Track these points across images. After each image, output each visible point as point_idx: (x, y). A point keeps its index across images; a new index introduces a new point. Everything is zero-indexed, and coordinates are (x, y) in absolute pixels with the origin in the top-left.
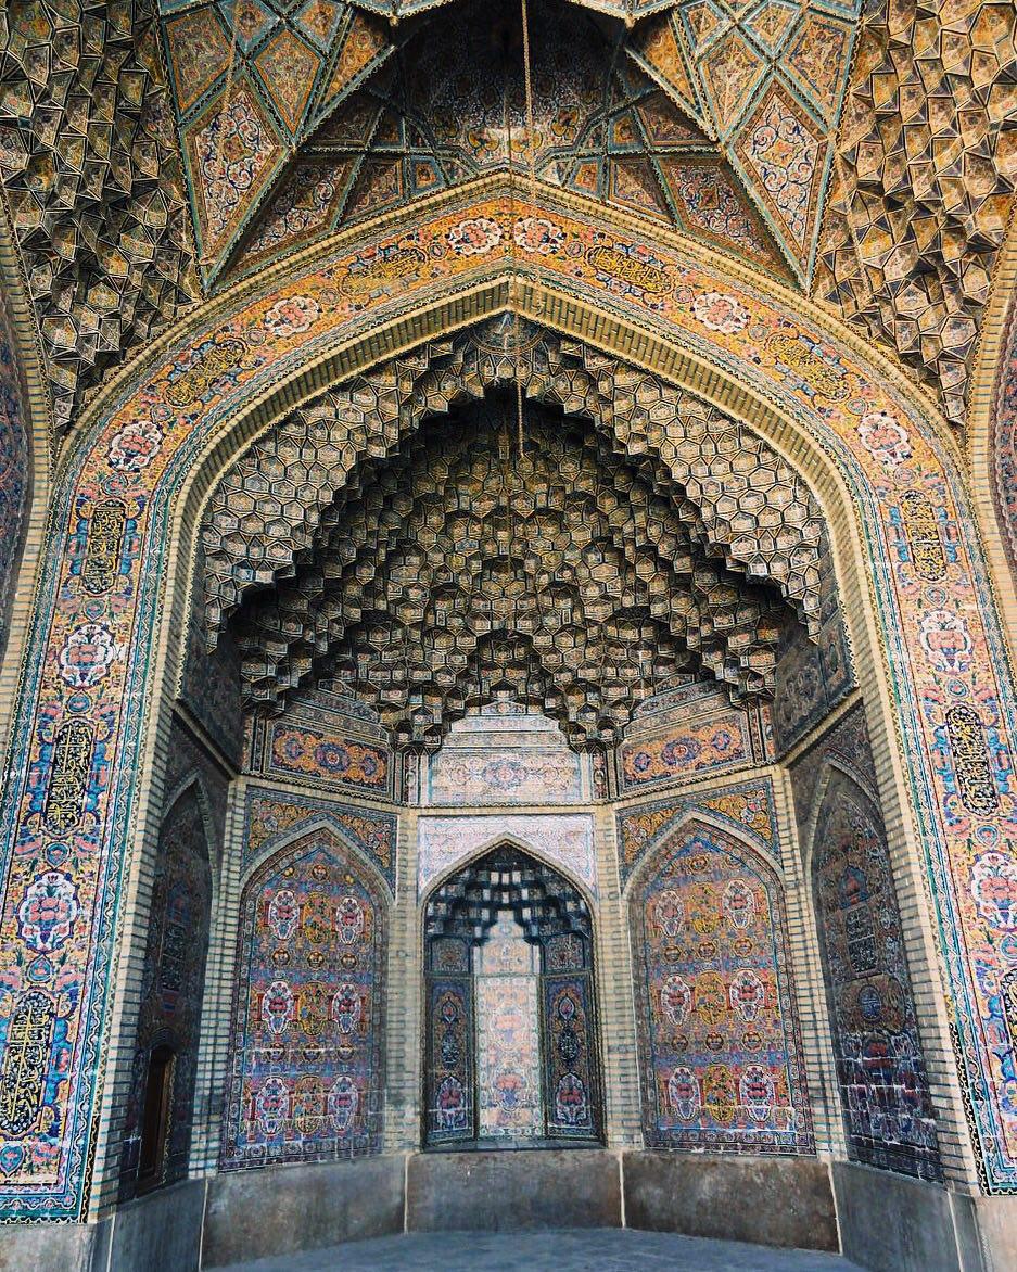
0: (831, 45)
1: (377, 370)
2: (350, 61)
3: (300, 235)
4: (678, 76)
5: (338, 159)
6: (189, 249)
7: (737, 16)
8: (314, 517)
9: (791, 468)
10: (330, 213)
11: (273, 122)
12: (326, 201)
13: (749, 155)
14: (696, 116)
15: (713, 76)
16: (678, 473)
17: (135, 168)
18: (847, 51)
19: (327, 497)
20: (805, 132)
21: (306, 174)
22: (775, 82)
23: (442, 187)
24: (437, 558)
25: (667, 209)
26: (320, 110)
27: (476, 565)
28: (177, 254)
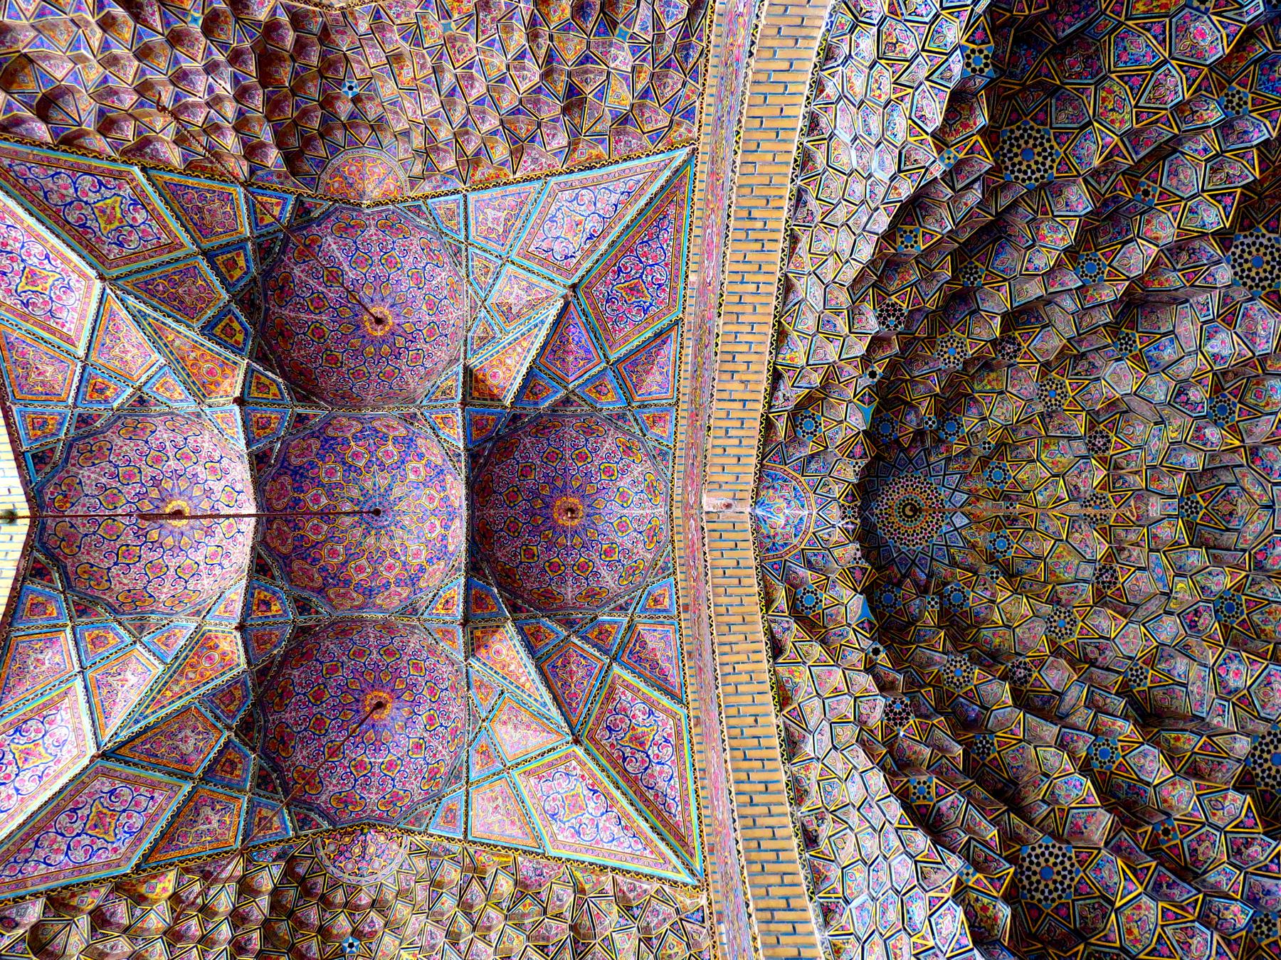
0: (488, 211)
2: (512, 668)
3: (678, 749)
4: (519, 350)
6: (657, 885)
8: (921, 841)
9: (818, 86)
12: (651, 713)
13: (575, 261)
14: (547, 326)
15: (519, 315)
16: (866, 252)
18: (486, 194)
19: (895, 809)
21: (610, 730)
22: (518, 254)
23: (672, 579)
24: (1169, 629)
25: (661, 336)
26: (544, 705)
27: (1196, 558)
28: (654, 901)
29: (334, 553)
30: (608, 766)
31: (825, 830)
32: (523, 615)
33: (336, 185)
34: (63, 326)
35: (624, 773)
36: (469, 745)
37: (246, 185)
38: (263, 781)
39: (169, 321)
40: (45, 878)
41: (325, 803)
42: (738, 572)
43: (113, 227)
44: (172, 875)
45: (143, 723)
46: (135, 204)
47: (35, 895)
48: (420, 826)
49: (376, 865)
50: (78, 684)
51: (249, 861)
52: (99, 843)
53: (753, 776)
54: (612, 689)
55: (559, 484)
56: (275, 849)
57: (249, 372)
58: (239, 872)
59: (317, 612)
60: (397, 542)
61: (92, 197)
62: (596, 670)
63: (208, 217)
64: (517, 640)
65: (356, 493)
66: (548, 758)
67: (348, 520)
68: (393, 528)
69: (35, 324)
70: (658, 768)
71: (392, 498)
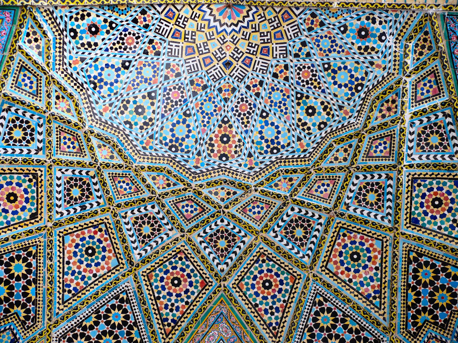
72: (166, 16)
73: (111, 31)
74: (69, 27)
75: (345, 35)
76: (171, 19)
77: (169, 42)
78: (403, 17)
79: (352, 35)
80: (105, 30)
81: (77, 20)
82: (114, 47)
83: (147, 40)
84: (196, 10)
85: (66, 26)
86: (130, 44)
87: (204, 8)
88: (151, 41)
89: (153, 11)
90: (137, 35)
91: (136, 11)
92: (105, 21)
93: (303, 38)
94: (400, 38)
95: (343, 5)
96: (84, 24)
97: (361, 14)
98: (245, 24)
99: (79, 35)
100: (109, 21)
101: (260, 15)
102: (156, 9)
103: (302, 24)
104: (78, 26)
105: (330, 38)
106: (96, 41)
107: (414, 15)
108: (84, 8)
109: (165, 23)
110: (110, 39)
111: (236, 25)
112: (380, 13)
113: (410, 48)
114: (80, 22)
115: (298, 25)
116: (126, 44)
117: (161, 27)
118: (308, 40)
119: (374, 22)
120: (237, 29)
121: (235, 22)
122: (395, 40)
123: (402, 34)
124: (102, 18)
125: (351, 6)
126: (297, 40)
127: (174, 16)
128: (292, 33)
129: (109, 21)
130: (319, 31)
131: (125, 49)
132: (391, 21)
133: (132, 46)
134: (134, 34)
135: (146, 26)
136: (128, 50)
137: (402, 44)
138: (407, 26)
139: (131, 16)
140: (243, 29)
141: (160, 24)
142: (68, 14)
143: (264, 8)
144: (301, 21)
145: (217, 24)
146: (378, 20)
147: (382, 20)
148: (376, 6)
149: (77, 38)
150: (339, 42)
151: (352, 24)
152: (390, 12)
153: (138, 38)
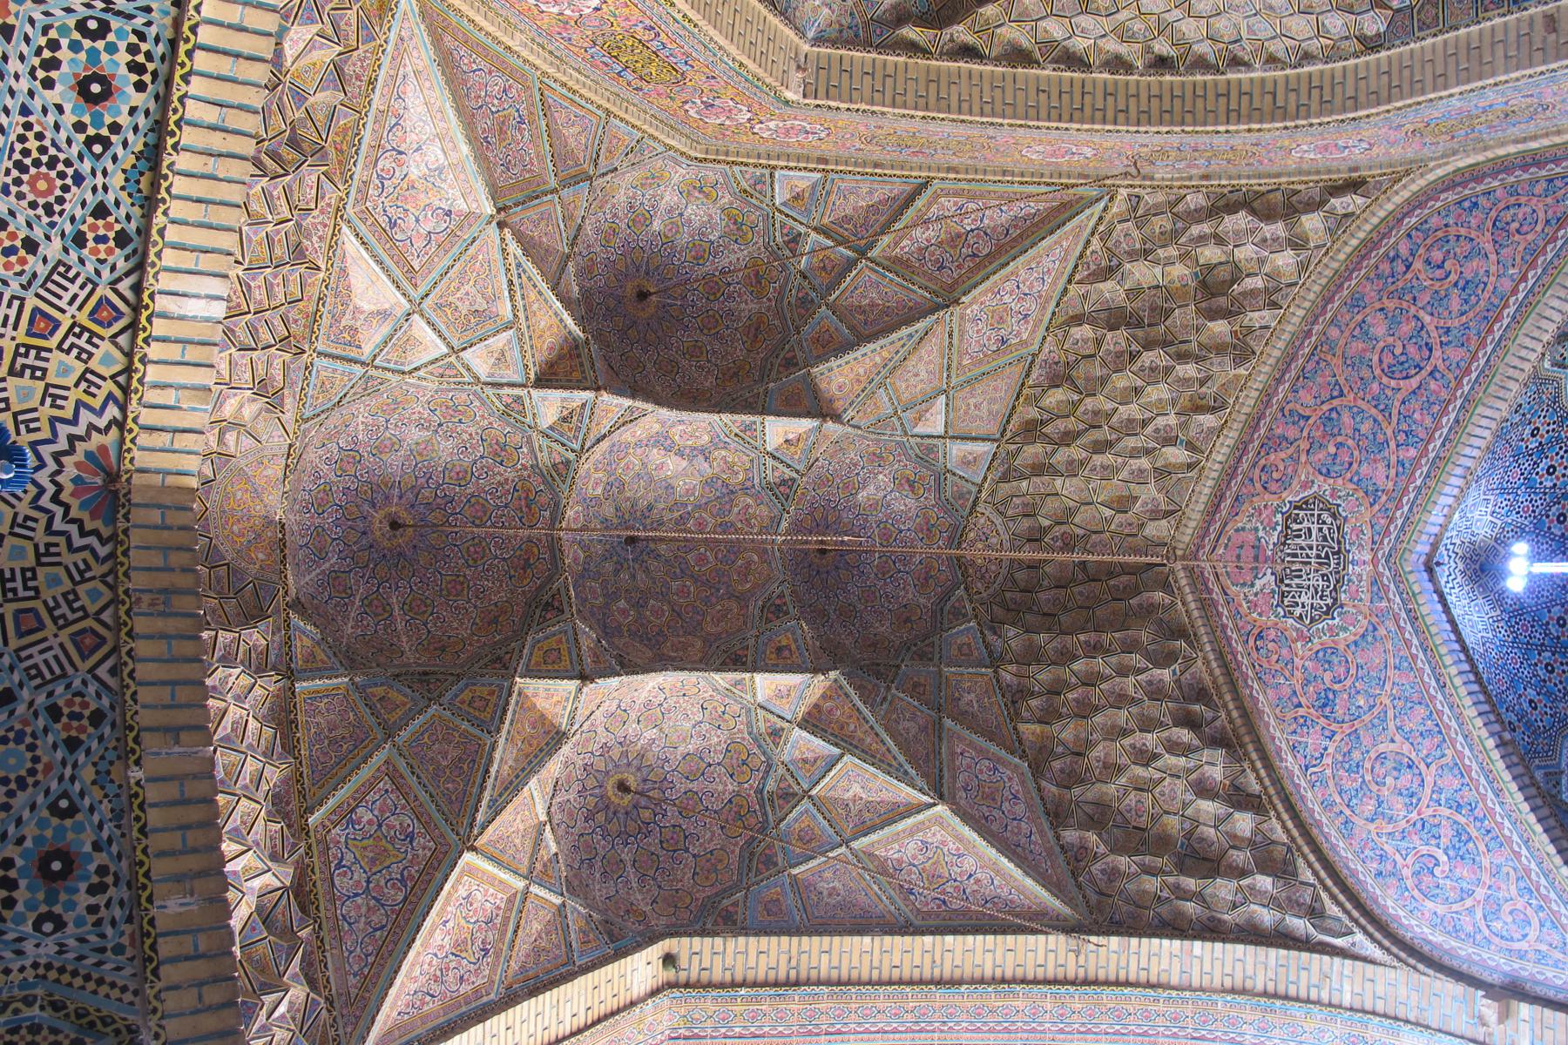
0: (344, 323)
1: (1018, 56)
2: (861, 371)
5: (898, 265)
6: (1095, 241)
7: (453, 359)
10: (929, 205)
11: (956, 334)
17: (1099, 342)
18: (326, 321)
20: (383, 221)
26: (911, 336)
28: (1109, 244)
29: (682, 591)
30: (982, 273)
31: (1162, 47)
32: (799, 354)
33: (261, 556)
34: (498, 908)
35: (991, 257)
36: (906, 434)
37: (290, 675)
38: (922, 656)
39: (493, 770)
40: (1042, 833)
41: (929, 599)
42: (879, 76)
43: (390, 847)
44: (1022, 727)
45: (907, 767)
46: (352, 822)
47: (1058, 838)
48: (970, 492)
49: (994, 540)
50: (860, 844)
51: (1001, 658)
52: (1007, 793)
53: (1100, 105)
54: (897, 260)
55: (612, 303)
56: (990, 637)
57: (531, 673)
58: (1013, 668)
59: (782, 596)
60: (667, 516)
61: (359, 875)
62: (873, 276)
63: (340, 731)
64: (833, 363)
65: (609, 567)
66: (955, 341)
67: (641, 576)
68: (648, 521)
69: (502, 940)
70: (986, 221)
71: (615, 521)
72: (103, 302)
73: (82, 137)
74: (115, 23)
75: (45, 813)
76: (92, 313)
77: (22, 300)
78: (118, 969)
79: (49, 833)
80: (87, 119)
81: (133, 49)
82: (30, 135)
83: (38, 233)
84: (109, 386)
85: (119, 13)
86: (32, 184)
87: (113, 411)
88: (31, 246)
89: (122, 266)
90: (57, 208)
91: (128, 217)
92: (115, 128)
93: (25, 694)
94: (53, 975)
95: (136, 795)
96: (117, 64)
97: (115, 849)
98: (58, 525)
99: (87, 43)
100: (114, 138)
101: (89, 568)
102: (127, 274)
103: (68, 686)
104: (112, 49)
105: (32, 772)
106: (59, 87)
107: (128, 997)
108: (161, 79)
109: (83, 295)
110: (57, 127)
111: (55, 499)
112: (122, 903)
113: (27, 1012)
114: (123, 57)
115: (64, 675)
116: (33, 171)
117: (72, 281)
118: (21, 709)
119: (92, 890)
120: (45, 502)
121: (64, 496)
122: (43, 961)
123: (66, 978)
124: (124, 120)
125: (138, 819)
126: (16, 677)
127: (100, 323)
128: (38, 659)
129: (114, 138)
130: (50, 739)
131: (20, 166)
132: (103, 936)
133: (25, 188)
134: (60, 200)
135: (80, 239)
136: (15, 173)
137: (34, 986)
138: (91, 986)
139: (117, 204)
140: (43, 518)
141: (80, 281)
142: (153, 30)
143: (110, 579)
144: (77, 683)
145: (62, 444)
146: (100, 900)
147: (103, 912)
148: (144, 887)
149: (76, 36)
150: (22, 798)
151: (79, 829)
152: (128, 928)
153: (49, 210)
